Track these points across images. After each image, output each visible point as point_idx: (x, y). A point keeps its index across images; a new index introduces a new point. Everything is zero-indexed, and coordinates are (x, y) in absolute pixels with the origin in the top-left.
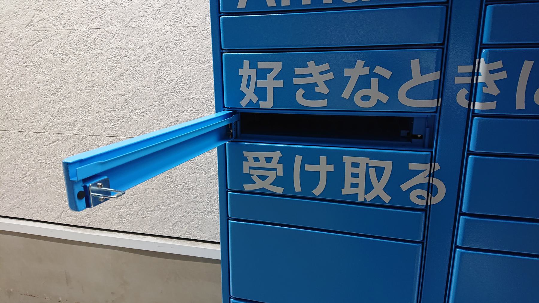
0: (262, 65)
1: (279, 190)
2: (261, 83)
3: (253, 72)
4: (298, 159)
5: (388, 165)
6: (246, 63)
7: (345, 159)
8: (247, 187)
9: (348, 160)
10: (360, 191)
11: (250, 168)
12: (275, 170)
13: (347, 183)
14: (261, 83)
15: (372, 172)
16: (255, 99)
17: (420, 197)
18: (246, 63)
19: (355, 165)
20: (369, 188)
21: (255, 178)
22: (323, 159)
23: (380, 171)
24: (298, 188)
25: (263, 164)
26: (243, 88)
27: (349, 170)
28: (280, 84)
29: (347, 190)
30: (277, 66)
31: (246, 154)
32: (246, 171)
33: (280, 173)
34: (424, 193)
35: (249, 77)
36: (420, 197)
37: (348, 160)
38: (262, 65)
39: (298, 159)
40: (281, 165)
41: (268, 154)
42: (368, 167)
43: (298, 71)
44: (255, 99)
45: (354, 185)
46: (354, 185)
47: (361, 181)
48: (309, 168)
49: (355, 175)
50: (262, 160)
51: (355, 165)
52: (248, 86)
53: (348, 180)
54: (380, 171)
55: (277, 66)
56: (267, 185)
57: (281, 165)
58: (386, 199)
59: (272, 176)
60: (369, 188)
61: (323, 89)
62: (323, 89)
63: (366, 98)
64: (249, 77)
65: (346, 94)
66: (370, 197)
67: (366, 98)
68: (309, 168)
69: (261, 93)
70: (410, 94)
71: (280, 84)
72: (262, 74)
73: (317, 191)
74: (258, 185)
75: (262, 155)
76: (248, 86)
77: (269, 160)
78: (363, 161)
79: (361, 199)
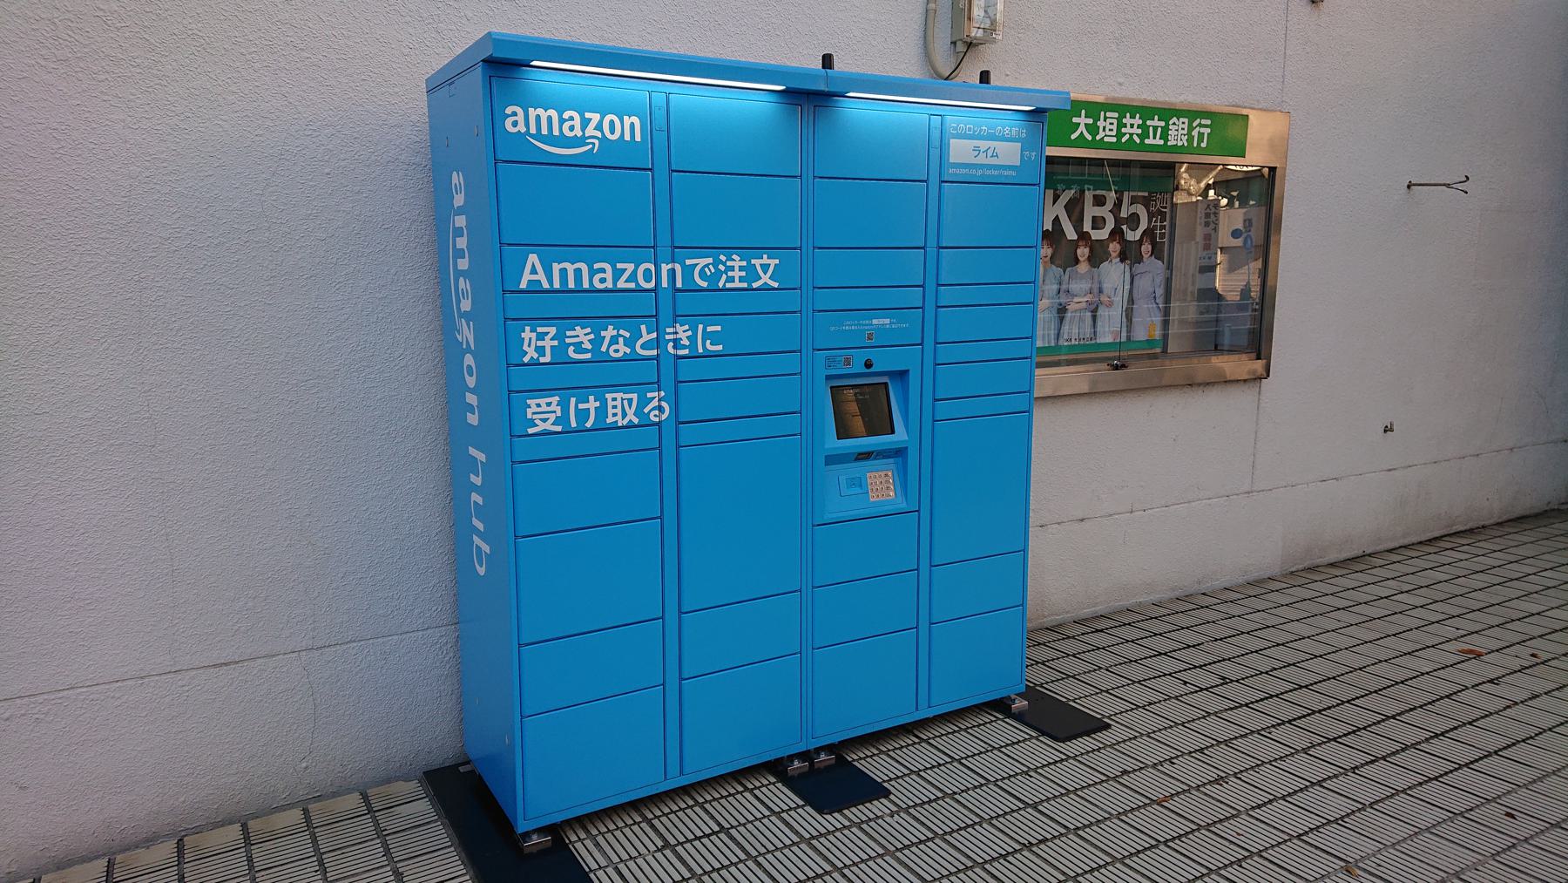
0: (540, 330)
1: (559, 429)
2: (540, 343)
3: (534, 335)
4: (573, 400)
5: (634, 396)
6: (527, 328)
7: (607, 396)
8: (531, 431)
9: (609, 396)
10: (619, 418)
11: (534, 413)
12: (555, 412)
13: (610, 415)
14: (540, 343)
15: (626, 403)
16: (535, 356)
17: (655, 416)
18: (527, 328)
19: (614, 399)
20: (624, 415)
21: (537, 422)
22: (591, 398)
23: (630, 401)
24: (574, 424)
25: (544, 408)
26: (525, 347)
27: (610, 404)
28: (555, 343)
29: (610, 420)
30: (553, 331)
31: (529, 402)
32: (529, 416)
33: (559, 414)
34: (657, 412)
35: (530, 339)
36: (655, 416)
37: (609, 396)
38: (540, 330)
39: (573, 400)
40: (559, 407)
41: (548, 400)
42: (622, 399)
43: (568, 333)
44: (535, 356)
45: (615, 415)
46: (615, 415)
47: (619, 411)
48: (581, 406)
49: (614, 407)
50: (544, 405)
51: (614, 399)
52: (529, 346)
53: (611, 411)
54: (630, 401)
55: (553, 331)
56: (548, 426)
57: (559, 407)
58: (636, 421)
59: (552, 417)
60: (624, 415)
61: (588, 346)
62: (588, 346)
63: (617, 351)
64: (530, 339)
65: (604, 349)
66: (625, 422)
67: (617, 351)
68: (581, 406)
69: (541, 351)
70: (643, 347)
71: (555, 343)
72: (541, 337)
73: (589, 425)
74: (541, 427)
75: (543, 401)
76: (529, 346)
77: (549, 404)
78: (619, 396)
79: (620, 424)
